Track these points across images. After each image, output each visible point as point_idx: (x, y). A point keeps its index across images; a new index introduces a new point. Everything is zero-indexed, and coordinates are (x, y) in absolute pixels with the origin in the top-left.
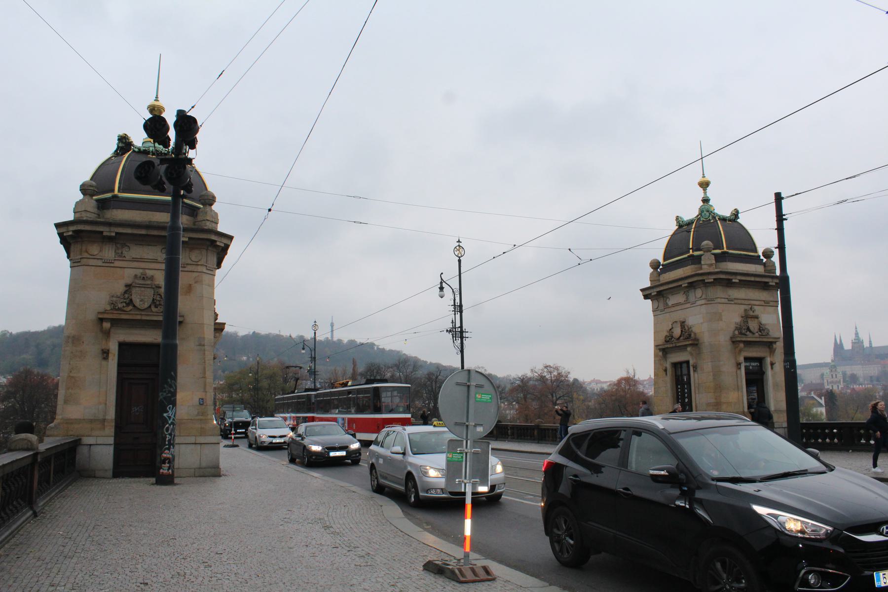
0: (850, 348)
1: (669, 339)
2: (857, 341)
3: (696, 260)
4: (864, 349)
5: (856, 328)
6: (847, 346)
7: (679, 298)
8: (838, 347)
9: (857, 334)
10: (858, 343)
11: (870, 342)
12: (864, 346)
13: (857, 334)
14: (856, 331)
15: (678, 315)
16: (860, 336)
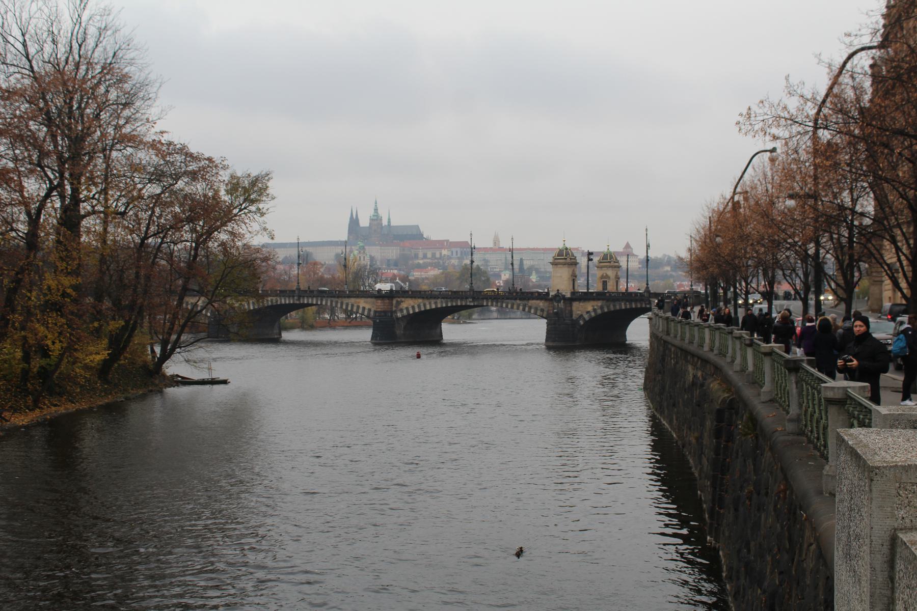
0: (367, 225)
1: (602, 276)
2: (375, 218)
3: (610, 262)
4: (382, 227)
5: (376, 203)
6: (364, 222)
7: (605, 269)
8: (354, 222)
9: (376, 210)
10: (377, 220)
11: (389, 219)
12: (382, 224)
13: (376, 210)
14: (376, 206)
15: (605, 272)
16: (379, 211)
